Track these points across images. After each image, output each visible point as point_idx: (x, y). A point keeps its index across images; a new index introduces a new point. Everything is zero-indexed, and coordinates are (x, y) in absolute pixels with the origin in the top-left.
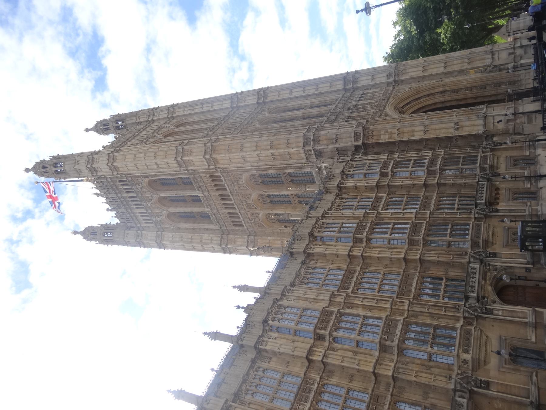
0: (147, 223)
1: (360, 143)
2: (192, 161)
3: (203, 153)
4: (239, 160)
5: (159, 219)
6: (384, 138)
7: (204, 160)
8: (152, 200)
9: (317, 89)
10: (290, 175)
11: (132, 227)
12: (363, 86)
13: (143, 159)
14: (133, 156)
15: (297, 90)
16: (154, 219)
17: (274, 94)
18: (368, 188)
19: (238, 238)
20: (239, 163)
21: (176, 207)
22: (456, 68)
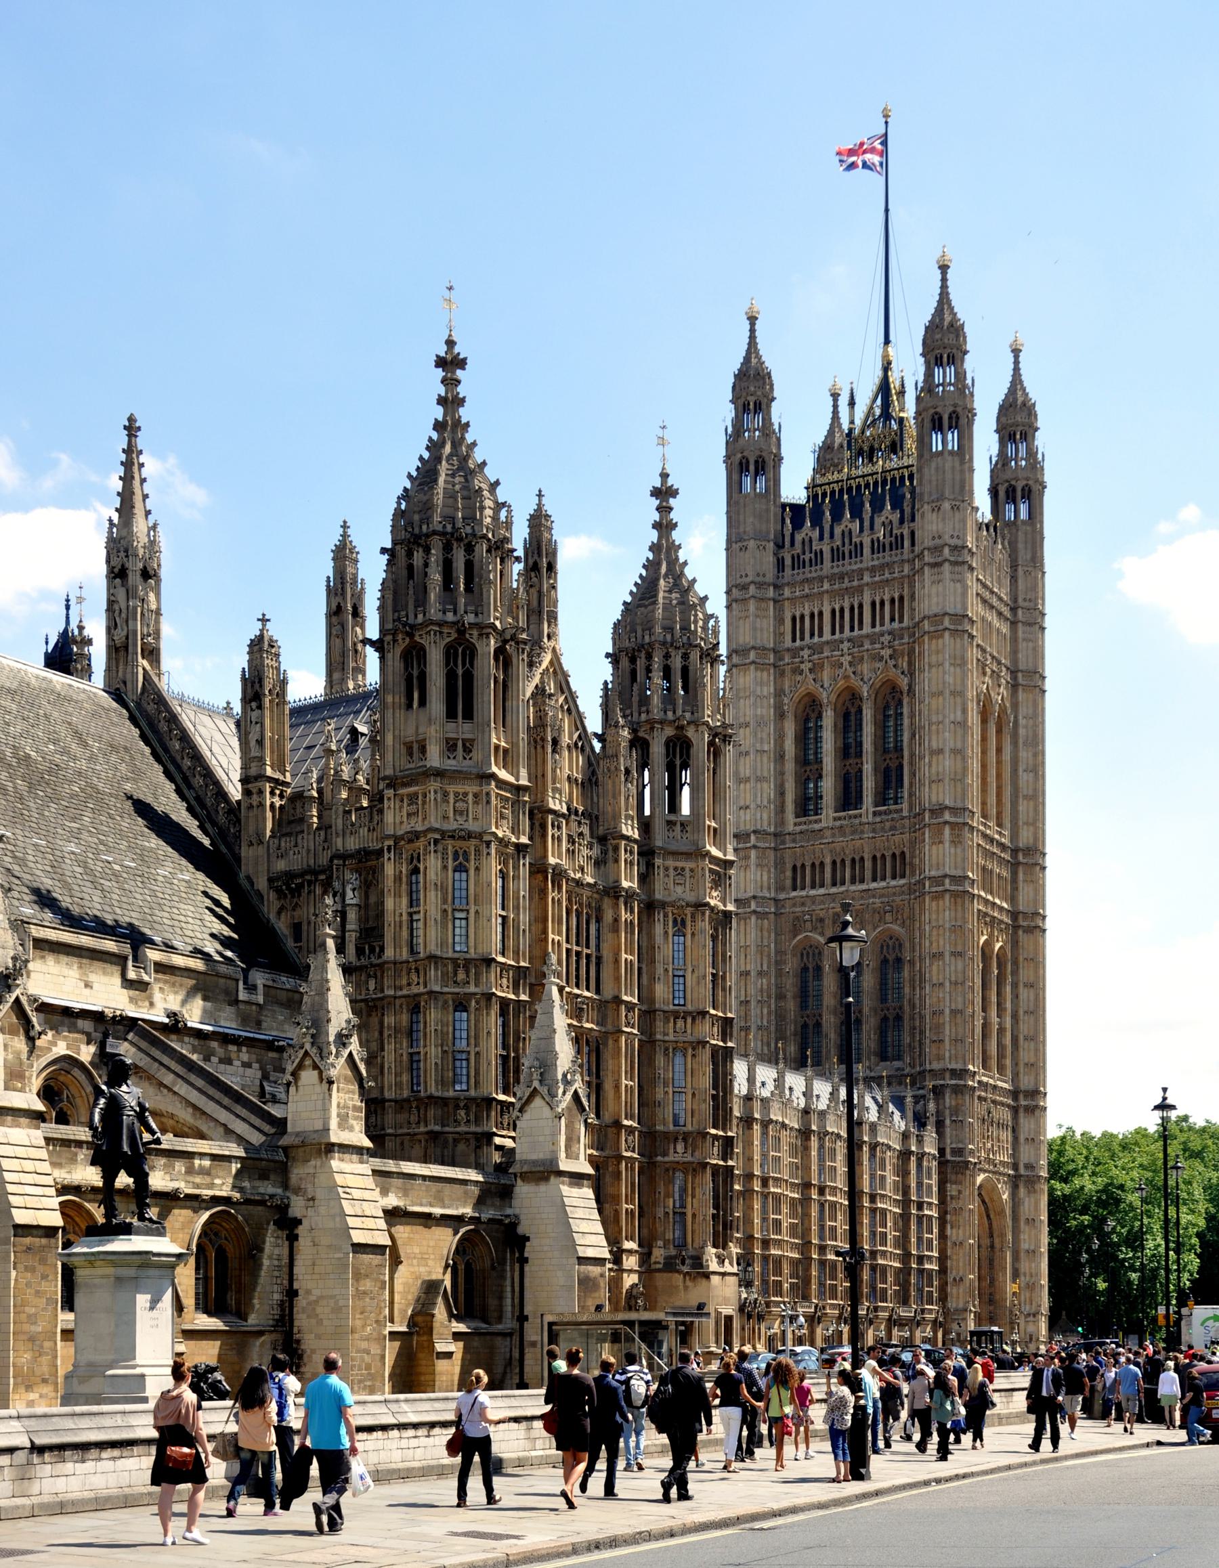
0: (794, 619)
1: (949, 1157)
2: (941, 842)
3: (953, 873)
4: (934, 945)
5: (806, 667)
6: (952, 1189)
7: (940, 873)
8: (854, 673)
9: (1026, 1039)
10: (899, 1018)
11: (780, 565)
12: (1017, 1123)
13: (952, 718)
14: (958, 688)
15: (1032, 998)
16: (806, 657)
17: (1031, 948)
18: (906, 1191)
19: (769, 871)
20: (931, 943)
21: (835, 725)
22: (1024, 1266)
